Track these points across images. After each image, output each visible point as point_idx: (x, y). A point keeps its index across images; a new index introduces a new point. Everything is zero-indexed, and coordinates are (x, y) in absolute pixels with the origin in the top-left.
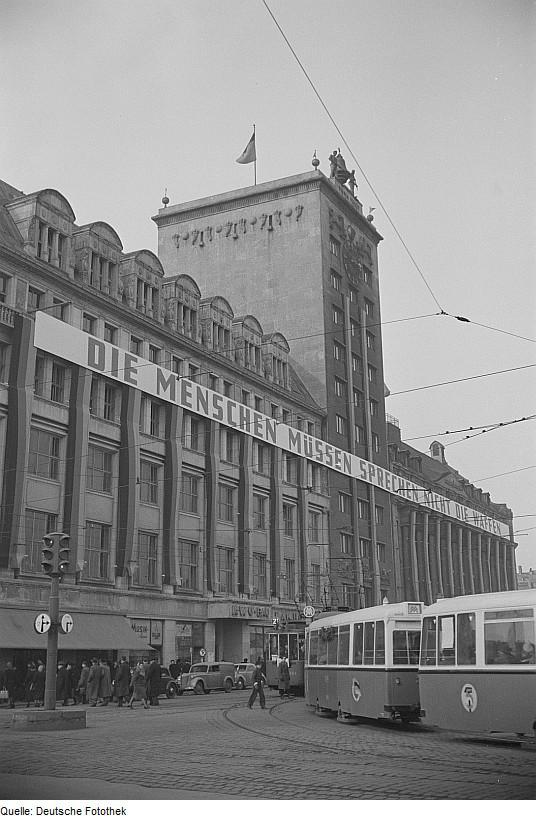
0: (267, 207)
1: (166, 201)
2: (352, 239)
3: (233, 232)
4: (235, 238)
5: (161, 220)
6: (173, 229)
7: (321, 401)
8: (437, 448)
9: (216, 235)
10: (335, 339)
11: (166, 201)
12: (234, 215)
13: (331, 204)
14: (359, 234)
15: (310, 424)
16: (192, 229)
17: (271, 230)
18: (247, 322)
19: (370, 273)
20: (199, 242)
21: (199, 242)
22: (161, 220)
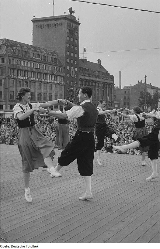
0: (56, 22)
1: (34, 16)
2: (73, 27)
3: (48, 26)
4: (48, 28)
5: (34, 21)
6: (36, 24)
7: (64, 64)
8: (99, 61)
9: (45, 26)
10: (68, 49)
11: (34, 16)
12: (49, 23)
13: (68, 22)
14: (74, 25)
15: (62, 69)
16: (40, 24)
17: (56, 27)
18: (49, 53)
19: (77, 33)
20: (41, 28)
21: (41, 28)
22: (34, 21)
